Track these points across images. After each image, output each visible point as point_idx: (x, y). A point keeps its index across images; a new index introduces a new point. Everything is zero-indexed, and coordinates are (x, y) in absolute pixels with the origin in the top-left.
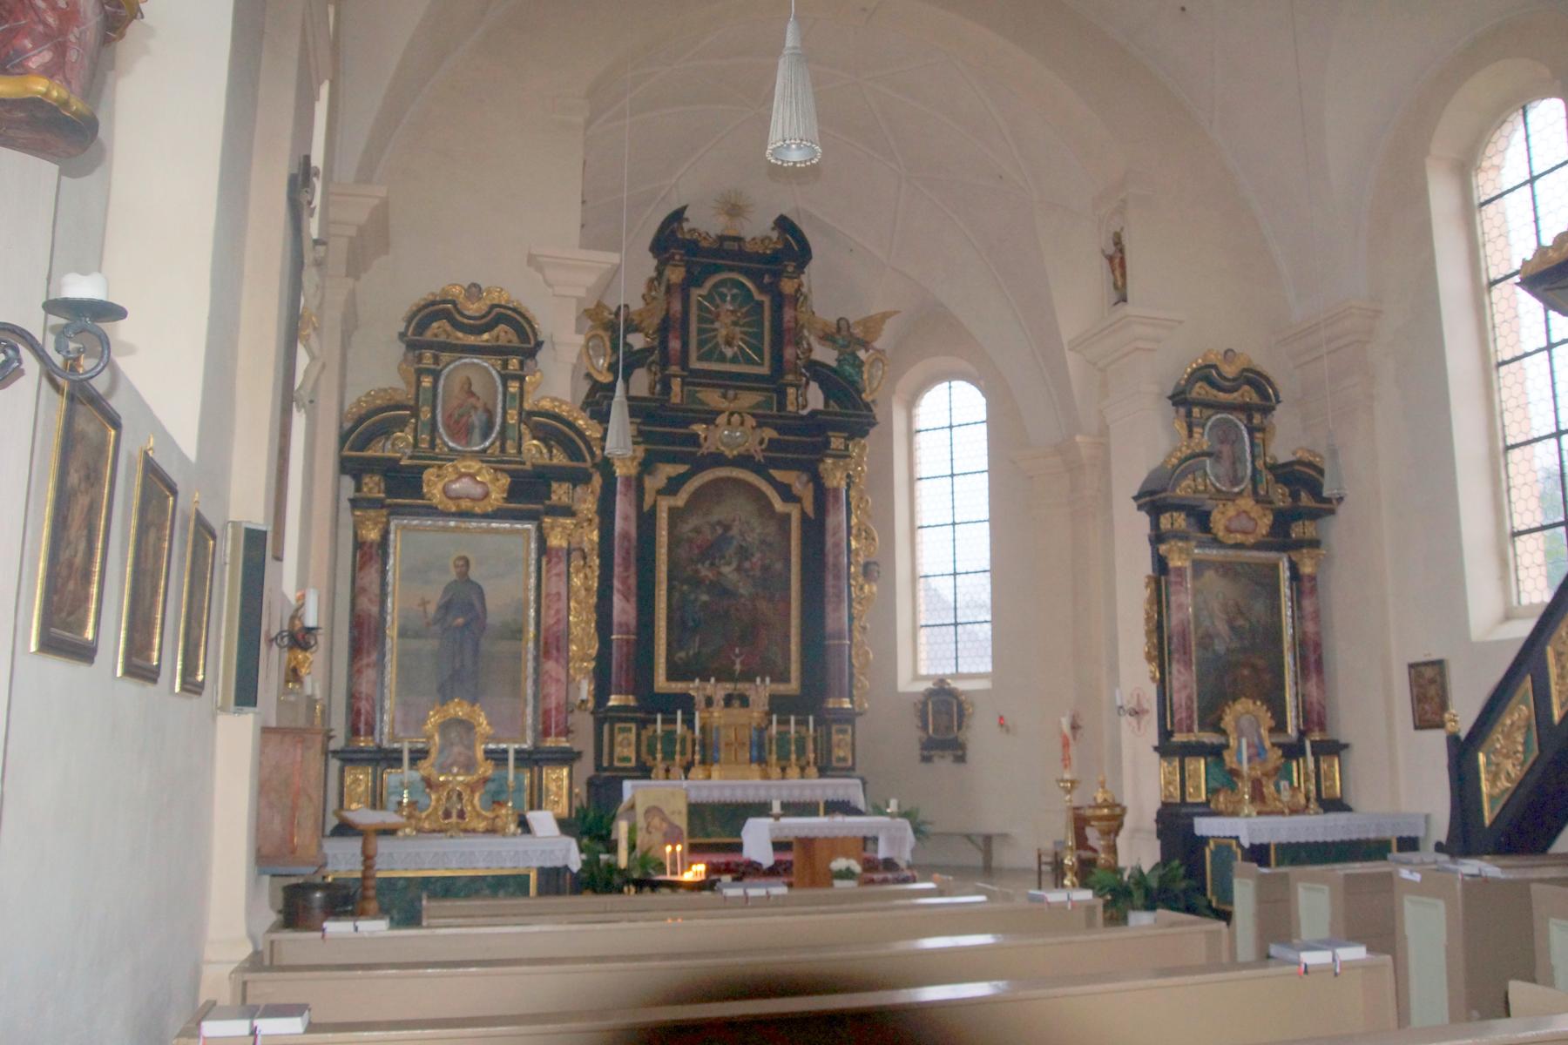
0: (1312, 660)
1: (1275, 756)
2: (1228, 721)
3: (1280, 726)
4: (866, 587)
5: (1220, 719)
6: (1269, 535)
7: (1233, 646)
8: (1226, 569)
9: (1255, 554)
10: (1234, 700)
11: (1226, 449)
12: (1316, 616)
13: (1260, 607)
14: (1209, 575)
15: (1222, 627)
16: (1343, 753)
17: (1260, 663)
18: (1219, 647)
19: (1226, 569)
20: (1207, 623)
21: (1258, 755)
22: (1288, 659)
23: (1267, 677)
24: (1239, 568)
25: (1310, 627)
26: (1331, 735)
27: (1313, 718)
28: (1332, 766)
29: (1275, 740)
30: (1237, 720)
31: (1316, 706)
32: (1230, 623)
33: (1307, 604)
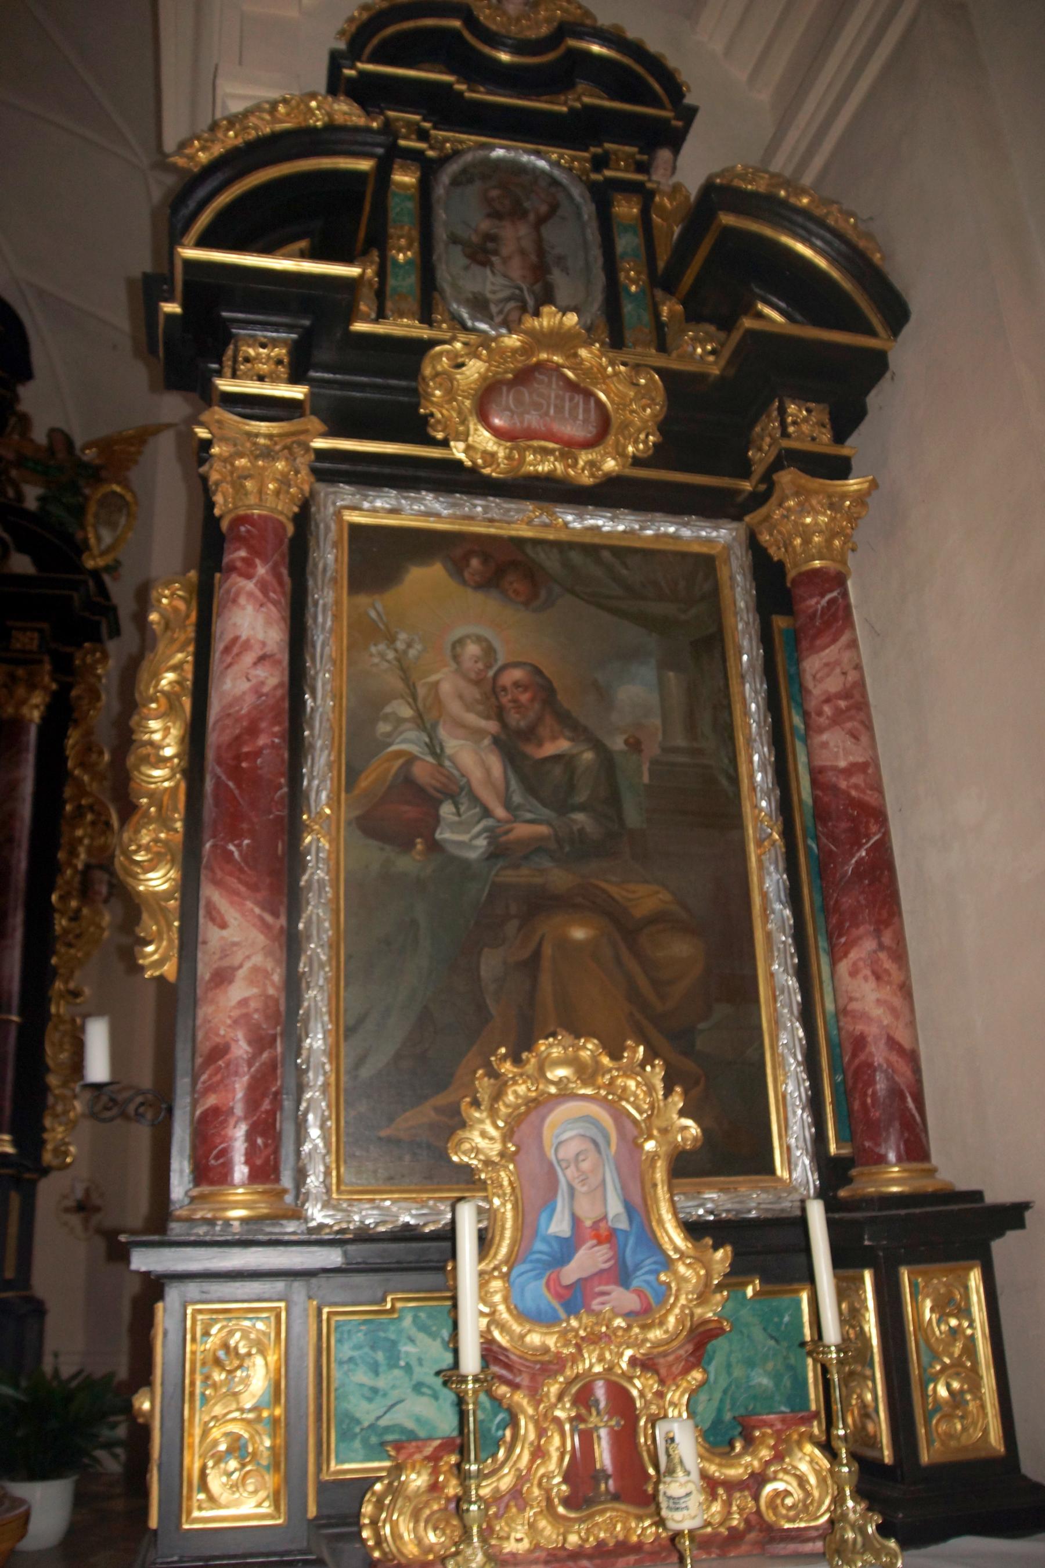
0: (849, 869)
1: (691, 1278)
2: (481, 1140)
3: (735, 1144)
4: (85, 911)
5: (455, 1123)
6: (658, 457)
7: (522, 830)
8: (503, 568)
9: (608, 524)
10: (521, 1046)
11: (514, 236)
12: (854, 705)
13: (639, 696)
14: (425, 577)
15: (474, 760)
16: (1004, 1248)
17: (645, 897)
18: (463, 836)
19: (503, 568)
20: (409, 742)
21: (620, 1274)
22: (768, 881)
23: (681, 949)
24: (551, 562)
25: (837, 749)
26: (953, 1166)
27: (872, 1101)
28: (952, 1305)
29: (712, 1201)
30: (523, 1125)
31: (879, 1054)
32: (511, 745)
33: (821, 671)
